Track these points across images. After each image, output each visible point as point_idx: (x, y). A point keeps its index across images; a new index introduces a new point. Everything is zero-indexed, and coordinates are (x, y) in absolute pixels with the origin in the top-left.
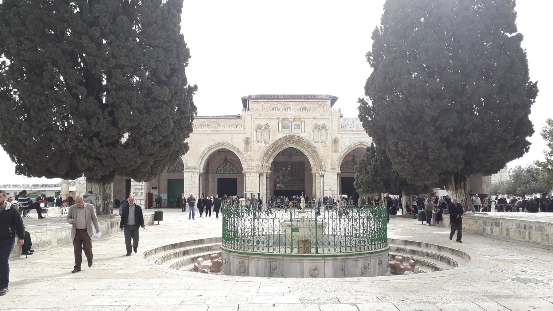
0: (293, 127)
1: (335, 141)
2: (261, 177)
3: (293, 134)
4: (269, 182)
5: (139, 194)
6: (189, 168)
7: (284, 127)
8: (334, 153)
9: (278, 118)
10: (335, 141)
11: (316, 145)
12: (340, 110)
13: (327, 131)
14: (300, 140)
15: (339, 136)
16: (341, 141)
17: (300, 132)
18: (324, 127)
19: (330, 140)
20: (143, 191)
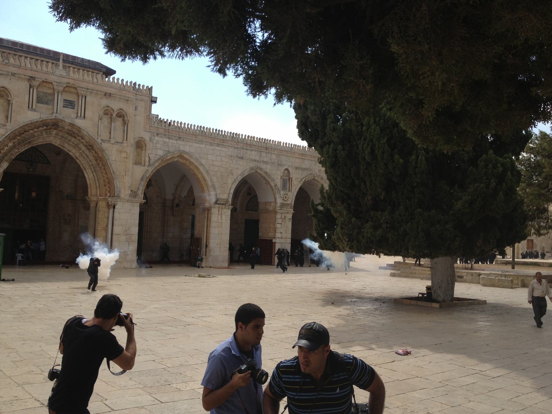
0: (61, 104)
1: (140, 145)
3: (60, 117)
7: (39, 101)
8: (135, 167)
9: (32, 78)
10: (140, 145)
11: (105, 146)
12: (150, 89)
13: (125, 123)
14: (74, 133)
15: (146, 136)
16: (149, 145)
17: (73, 116)
18: (121, 115)
19: (132, 140)
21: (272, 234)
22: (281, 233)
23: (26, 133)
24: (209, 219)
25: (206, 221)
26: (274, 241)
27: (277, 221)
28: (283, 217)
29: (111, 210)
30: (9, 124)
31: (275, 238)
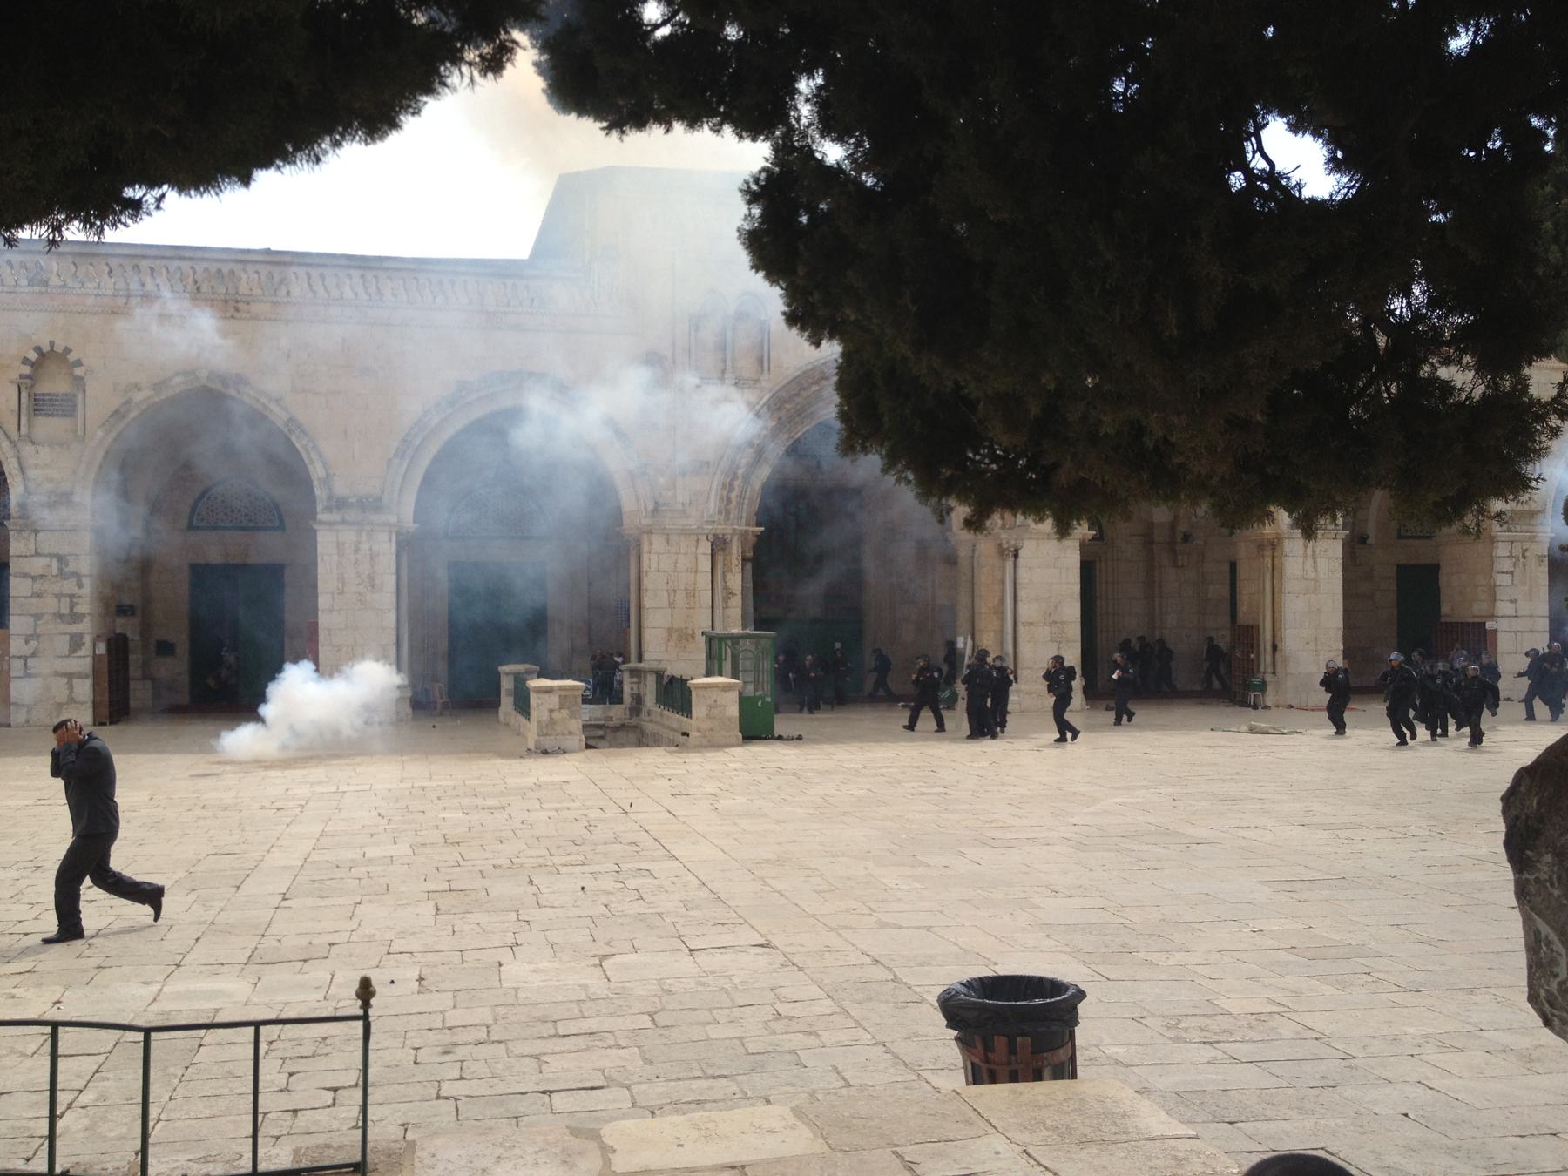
2: (719, 558)
4: (750, 585)
5: (63, 644)
6: (340, 504)
20: (85, 627)
21: (1485, 605)
22: (1514, 601)
23: (804, 394)
24: (1276, 570)
25: (1268, 576)
26: (1489, 625)
27: (1498, 567)
28: (1517, 550)
29: (1009, 564)
30: (765, 376)
31: (1492, 616)
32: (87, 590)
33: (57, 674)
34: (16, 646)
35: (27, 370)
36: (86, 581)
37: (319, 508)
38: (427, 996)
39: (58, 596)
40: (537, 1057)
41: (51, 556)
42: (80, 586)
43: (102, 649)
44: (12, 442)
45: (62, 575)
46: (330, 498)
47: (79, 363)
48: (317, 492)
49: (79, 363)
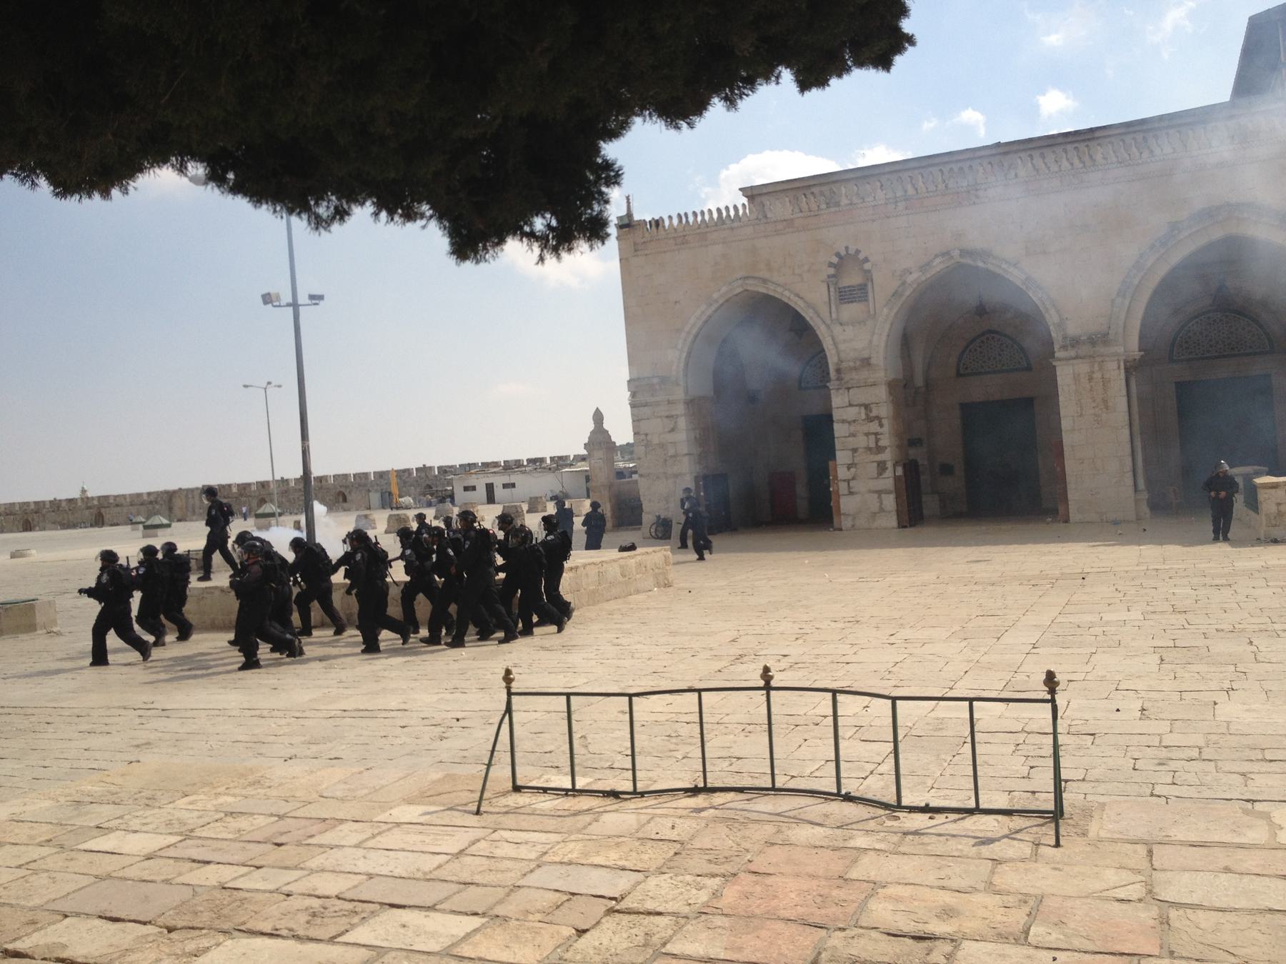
5: (873, 469)
6: (1075, 342)
20: (887, 456)
32: (886, 429)
33: (870, 491)
34: (842, 473)
35: (832, 271)
36: (885, 422)
37: (1056, 347)
38: (1147, 722)
39: (867, 434)
40: (1243, 774)
41: (860, 405)
42: (881, 425)
43: (900, 471)
44: (828, 327)
45: (870, 419)
46: (1065, 338)
47: (866, 260)
48: (1054, 335)
49: (866, 260)
